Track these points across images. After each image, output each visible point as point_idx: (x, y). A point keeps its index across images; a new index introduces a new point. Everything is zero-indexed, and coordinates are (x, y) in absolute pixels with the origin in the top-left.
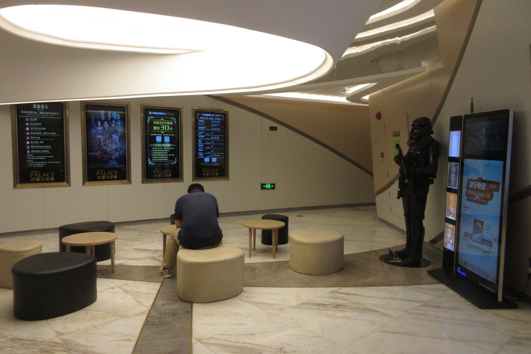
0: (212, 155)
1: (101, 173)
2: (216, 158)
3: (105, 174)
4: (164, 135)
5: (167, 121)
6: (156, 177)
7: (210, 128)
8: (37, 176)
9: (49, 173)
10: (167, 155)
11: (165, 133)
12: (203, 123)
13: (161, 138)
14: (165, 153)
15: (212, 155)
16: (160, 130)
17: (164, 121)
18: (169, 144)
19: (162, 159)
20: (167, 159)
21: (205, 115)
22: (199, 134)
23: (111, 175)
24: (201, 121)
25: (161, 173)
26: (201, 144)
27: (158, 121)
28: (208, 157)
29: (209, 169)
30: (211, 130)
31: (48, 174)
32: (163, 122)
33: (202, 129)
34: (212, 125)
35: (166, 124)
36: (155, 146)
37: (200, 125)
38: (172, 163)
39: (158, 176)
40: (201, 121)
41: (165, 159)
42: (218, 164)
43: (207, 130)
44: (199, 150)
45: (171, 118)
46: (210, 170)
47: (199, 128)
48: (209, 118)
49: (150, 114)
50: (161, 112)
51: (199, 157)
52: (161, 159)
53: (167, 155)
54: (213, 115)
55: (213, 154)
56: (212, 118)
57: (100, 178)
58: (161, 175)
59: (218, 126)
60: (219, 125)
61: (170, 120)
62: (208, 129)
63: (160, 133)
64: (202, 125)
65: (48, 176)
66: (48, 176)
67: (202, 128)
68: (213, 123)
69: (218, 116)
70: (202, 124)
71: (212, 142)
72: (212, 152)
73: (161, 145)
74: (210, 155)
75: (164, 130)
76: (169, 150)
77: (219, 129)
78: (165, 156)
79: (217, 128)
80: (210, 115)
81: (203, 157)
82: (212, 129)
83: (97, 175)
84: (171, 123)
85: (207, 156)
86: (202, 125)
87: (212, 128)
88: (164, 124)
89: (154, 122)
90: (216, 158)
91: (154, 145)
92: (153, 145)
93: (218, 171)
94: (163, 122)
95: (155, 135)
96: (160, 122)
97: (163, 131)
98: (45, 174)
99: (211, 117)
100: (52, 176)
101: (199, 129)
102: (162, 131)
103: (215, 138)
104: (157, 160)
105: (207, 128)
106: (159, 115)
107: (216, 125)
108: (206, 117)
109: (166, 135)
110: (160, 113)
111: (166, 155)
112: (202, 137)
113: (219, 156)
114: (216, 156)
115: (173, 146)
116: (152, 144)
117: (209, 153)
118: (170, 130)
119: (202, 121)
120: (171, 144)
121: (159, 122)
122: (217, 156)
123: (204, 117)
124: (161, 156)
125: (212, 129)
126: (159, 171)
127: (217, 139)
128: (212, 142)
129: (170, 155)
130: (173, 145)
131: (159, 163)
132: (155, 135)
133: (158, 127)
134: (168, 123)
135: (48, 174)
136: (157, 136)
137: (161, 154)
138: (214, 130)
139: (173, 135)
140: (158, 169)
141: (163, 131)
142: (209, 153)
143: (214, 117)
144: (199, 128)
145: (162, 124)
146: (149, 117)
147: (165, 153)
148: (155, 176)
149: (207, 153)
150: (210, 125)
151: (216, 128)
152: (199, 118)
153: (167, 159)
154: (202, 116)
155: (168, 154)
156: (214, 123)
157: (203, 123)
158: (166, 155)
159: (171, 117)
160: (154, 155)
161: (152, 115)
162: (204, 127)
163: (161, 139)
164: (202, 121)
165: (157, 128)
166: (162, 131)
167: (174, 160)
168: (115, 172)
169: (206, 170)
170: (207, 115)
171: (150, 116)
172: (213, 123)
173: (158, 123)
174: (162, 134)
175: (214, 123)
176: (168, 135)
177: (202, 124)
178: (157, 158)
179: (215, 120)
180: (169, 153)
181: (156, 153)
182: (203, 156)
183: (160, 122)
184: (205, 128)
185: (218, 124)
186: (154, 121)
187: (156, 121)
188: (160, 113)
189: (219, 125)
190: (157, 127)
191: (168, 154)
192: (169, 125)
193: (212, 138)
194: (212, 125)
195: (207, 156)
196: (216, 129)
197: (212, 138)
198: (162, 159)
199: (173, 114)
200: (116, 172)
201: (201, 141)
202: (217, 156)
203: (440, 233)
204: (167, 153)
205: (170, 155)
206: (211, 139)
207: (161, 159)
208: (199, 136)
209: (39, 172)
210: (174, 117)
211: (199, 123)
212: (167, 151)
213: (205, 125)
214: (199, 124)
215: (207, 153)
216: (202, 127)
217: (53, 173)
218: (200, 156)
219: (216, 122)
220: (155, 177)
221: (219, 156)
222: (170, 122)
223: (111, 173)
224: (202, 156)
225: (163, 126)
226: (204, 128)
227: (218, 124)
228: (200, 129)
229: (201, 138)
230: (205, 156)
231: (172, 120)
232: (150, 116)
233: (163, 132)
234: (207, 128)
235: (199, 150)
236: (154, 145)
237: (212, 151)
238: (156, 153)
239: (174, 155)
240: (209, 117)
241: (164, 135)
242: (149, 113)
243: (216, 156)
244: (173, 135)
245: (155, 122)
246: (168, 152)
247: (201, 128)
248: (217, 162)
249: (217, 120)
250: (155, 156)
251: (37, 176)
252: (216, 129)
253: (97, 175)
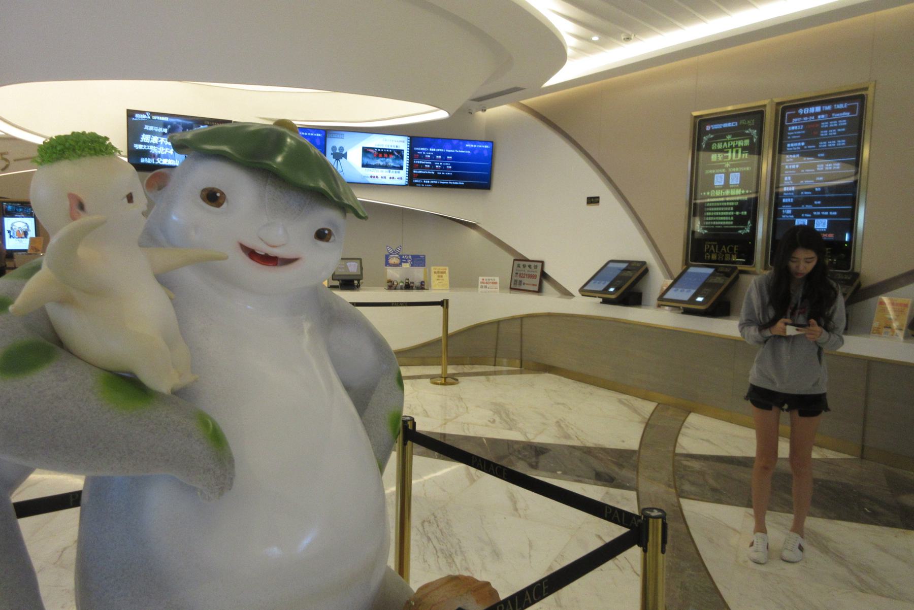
0: (815, 213)
1: (711, 249)
2: (826, 221)
3: (718, 251)
4: (730, 170)
5: (738, 140)
6: (707, 258)
7: (816, 143)
8: (714, 251)
9: (730, 247)
10: (732, 213)
11: (732, 166)
12: (799, 132)
13: (723, 177)
14: (729, 209)
15: (815, 213)
16: (723, 161)
17: (733, 140)
18: (737, 190)
19: (722, 223)
20: (731, 223)
21: (806, 111)
22: (786, 162)
23: (727, 253)
24: (793, 128)
25: (717, 251)
26: (789, 186)
27: (720, 142)
28: (805, 217)
29: (717, 246)
30: (817, 147)
31: (728, 248)
32: (730, 143)
33: (795, 149)
34: (824, 134)
35: (737, 146)
36: (711, 195)
37: (791, 139)
38: (740, 232)
39: (711, 258)
40: (793, 128)
41: (727, 223)
42: (831, 236)
43: (807, 148)
44: (784, 200)
45: (747, 132)
46: (720, 249)
47: (789, 145)
48: (816, 118)
49: (707, 129)
50: (728, 122)
51: (784, 216)
52: (719, 223)
53: (732, 213)
54: (828, 108)
55: (816, 210)
56: (823, 116)
57: (709, 257)
58: (718, 257)
59: (839, 133)
60: (844, 130)
61: (743, 136)
62: (809, 147)
63: (722, 167)
64: (794, 137)
65: (728, 251)
66: (728, 251)
67: (796, 144)
68: (824, 129)
69: (840, 106)
70: (796, 135)
71: (818, 179)
72: (818, 205)
73: (722, 192)
74: (810, 212)
75: (732, 160)
76: (792, 199)
77: (841, 143)
78: (728, 216)
79: (836, 139)
80: (818, 109)
81: (792, 216)
82: (823, 145)
83: (705, 250)
84: (747, 142)
85: (803, 215)
86: (794, 137)
87: (823, 140)
88: (732, 147)
89: (713, 145)
90: (826, 221)
91: (710, 194)
92: (708, 193)
93: (736, 251)
94: (730, 143)
95: (714, 171)
96: (725, 144)
97: (729, 161)
98: (724, 248)
99: (822, 112)
100: (733, 252)
101: (788, 149)
102: (726, 162)
103: (827, 168)
104: (713, 225)
105: (807, 143)
106: (723, 129)
107: (833, 133)
108: (809, 115)
109: (734, 169)
110: (726, 125)
111: (730, 213)
112: (794, 167)
113: (835, 213)
114: (819, 213)
115: (745, 192)
116: (706, 192)
117: (808, 207)
118: (743, 157)
119: (796, 128)
120: (742, 190)
121: (723, 145)
122: (831, 213)
123: (803, 115)
124: (721, 216)
125: (823, 145)
126: (715, 246)
127: (832, 170)
128: (818, 179)
129: (737, 213)
130: (745, 190)
131: (715, 229)
132: (714, 171)
133: (719, 155)
134: (740, 143)
135: (728, 248)
136: (717, 173)
137: (721, 211)
138: (836, 146)
139: (748, 169)
140: (714, 243)
141: (729, 161)
142: (808, 207)
143: (829, 113)
144: (786, 147)
145: (728, 148)
146: (756, 131)
147: (729, 209)
148: (707, 256)
149: (803, 207)
150: (818, 135)
151: (831, 139)
152: (790, 120)
153: (731, 223)
154: (797, 115)
155: (734, 211)
156: (828, 129)
157: (799, 132)
158: (730, 213)
159: (747, 129)
160: (708, 214)
161: (712, 131)
162: (801, 142)
163: (723, 180)
164: (796, 128)
165: (717, 157)
166: (726, 162)
167: (746, 224)
168: (733, 248)
169: (712, 246)
170: (812, 110)
171: (708, 134)
172: (824, 129)
173: (720, 146)
174: (727, 169)
175: (828, 129)
176: (737, 169)
177: (796, 135)
178: (713, 221)
179: (831, 120)
180: (736, 208)
181: (713, 209)
182: (791, 215)
183: (725, 144)
184: (803, 144)
185: (839, 130)
186: (712, 143)
187: (717, 143)
188: (726, 125)
189: (844, 130)
190: (717, 156)
191: (734, 211)
192: (741, 147)
193: (818, 169)
194: (824, 134)
195: (803, 215)
196: (832, 144)
197: (820, 167)
198: (722, 223)
199: (750, 122)
200: (737, 248)
201: (789, 178)
202: (831, 213)
203: (231, 446)
204: (732, 209)
205: (737, 213)
206: (817, 171)
207: (719, 223)
208: (787, 167)
209: (716, 243)
210: (753, 128)
211: (789, 134)
212: (732, 204)
213: (802, 137)
214: (789, 135)
215: (803, 207)
216: (794, 143)
217: (735, 246)
218: (785, 214)
219: (834, 124)
220: (706, 258)
221: (835, 213)
222: (743, 139)
223: (726, 250)
224: (788, 215)
225: (730, 150)
226: (799, 144)
227: (839, 130)
228: (791, 147)
229: (792, 169)
230: (798, 214)
231: (749, 134)
232: (707, 133)
233: (727, 165)
234: (807, 143)
235: (784, 200)
236: (710, 194)
237: (816, 202)
238: (713, 209)
239: (745, 213)
240: (816, 115)
241: (730, 170)
242: (705, 128)
243: (819, 213)
244: (748, 169)
245: (716, 144)
246: (734, 206)
247: (792, 145)
248: (828, 231)
249: (837, 120)
250: (709, 216)
251: (714, 251)
252: (832, 144)
253: (705, 250)
